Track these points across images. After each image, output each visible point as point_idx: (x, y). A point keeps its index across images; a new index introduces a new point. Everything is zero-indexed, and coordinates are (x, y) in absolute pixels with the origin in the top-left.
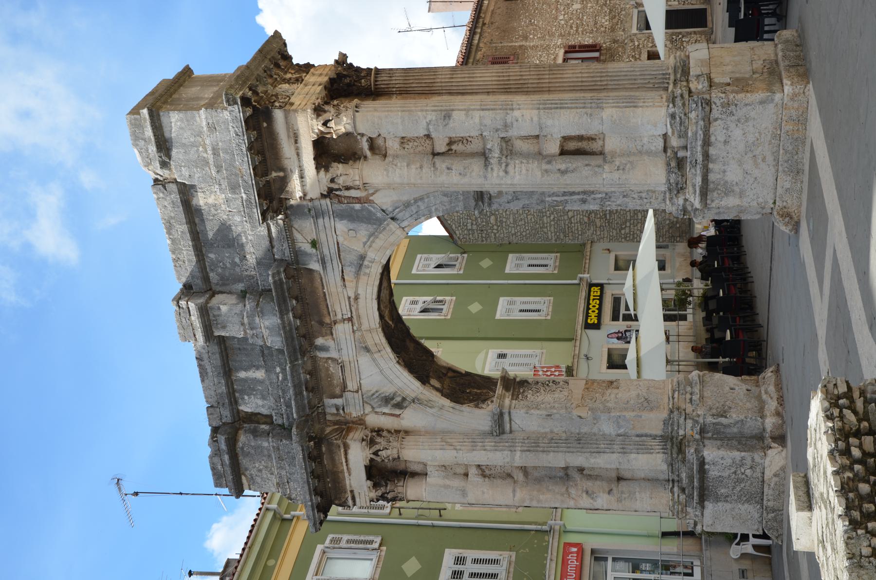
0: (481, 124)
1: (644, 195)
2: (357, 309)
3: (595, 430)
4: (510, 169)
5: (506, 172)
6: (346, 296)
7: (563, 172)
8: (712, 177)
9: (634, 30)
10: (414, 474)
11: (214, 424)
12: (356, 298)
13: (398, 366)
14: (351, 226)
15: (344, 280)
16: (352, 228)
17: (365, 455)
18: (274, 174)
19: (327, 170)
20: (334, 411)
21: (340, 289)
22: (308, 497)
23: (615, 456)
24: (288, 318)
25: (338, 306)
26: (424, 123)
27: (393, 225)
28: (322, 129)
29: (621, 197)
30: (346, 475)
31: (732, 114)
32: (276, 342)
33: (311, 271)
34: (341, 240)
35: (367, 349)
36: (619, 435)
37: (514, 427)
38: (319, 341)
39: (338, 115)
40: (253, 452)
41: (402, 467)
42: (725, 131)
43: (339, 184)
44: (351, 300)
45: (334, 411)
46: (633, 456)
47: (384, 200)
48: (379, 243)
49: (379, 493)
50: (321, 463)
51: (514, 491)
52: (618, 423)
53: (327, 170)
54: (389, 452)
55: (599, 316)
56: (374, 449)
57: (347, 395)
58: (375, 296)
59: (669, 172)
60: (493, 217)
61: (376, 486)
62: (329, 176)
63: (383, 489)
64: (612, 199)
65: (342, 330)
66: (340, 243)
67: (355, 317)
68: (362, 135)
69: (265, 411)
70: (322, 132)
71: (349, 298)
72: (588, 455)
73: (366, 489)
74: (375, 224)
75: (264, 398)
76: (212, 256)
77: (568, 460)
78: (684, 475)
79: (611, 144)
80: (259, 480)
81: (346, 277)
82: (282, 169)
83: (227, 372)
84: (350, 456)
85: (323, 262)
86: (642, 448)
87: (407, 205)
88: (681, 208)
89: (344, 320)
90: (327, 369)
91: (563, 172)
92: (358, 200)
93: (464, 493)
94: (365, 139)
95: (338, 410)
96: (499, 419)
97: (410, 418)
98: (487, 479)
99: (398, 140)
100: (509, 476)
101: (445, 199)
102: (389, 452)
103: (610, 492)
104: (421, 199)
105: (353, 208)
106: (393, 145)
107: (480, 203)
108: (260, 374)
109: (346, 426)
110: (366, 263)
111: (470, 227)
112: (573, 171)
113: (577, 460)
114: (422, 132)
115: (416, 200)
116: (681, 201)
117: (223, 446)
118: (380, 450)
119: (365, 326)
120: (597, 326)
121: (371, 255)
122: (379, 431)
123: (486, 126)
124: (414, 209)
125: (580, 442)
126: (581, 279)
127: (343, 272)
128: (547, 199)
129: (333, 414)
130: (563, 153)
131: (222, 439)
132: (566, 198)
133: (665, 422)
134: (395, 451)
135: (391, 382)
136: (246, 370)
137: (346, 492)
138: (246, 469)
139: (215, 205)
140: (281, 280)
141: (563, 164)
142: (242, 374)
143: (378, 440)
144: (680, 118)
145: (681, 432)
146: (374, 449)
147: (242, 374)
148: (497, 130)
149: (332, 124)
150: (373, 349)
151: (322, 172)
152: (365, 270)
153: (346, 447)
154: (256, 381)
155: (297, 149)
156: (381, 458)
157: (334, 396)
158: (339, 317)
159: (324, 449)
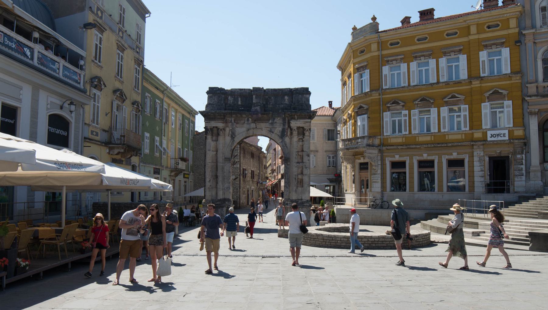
4: (296, 168)
5: (296, 167)
7: (295, 179)
9: (247, 187)
10: (212, 138)
14: (281, 131)
18: (296, 117)
19: (297, 129)
20: (230, 120)
23: (222, 187)
26: (307, 151)
27: (281, 141)
31: (308, 212)
33: (269, 120)
35: (248, 130)
38: (250, 119)
40: (220, 99)
41: (213, 135)
45: (230, 120)
46: (222, 191)
47: (287, 139)
49: (209, 129)
51: (210, 163)
53: (297, 129)
54: (221, 133)
55: (186, 178)
57: (235, 124)
59: (295, 200)
60: (203, 147)
61: (211, 129)
62: (295, 129)
63: (210, 130)
65: (253, 125)
68: (304, 137)
69: (229, 102)
70: (305, 129)
75: (233, 103)
76: (272, 98)
78: (218, 203)
80: (211, 99)
82: (297, 119)
84: (220, 123)
86: (224, 193)
87: (286, 144)
90: (242, 120)
91: (295, 179)
92: (287, 134)
93: (209, 150)
97: (228, 139)
101: (287, 152)
102: (221, 133)
103: (210, 186)
104: (287, 147)
108: (240, 103)
109: (226, 122)
110: (271, 133)
112: (296, 181)
113: (220, 179)
114: (304, 150)
115: (287, 147)
120: (184, 177)
121: (273, 135)
122: (225, 131)
126: (191, 172)
130: (298, 178)
136: (241, 100)
138: (214, 96)
139: (285, 101)
142: (240, 99)
145: (227, 202)
147: (240, 99)
150: (248, 132)
151: (296, 128)
153: (223, 123)
154: (238, 102)
157: (234, 121)
159: (222, 117)
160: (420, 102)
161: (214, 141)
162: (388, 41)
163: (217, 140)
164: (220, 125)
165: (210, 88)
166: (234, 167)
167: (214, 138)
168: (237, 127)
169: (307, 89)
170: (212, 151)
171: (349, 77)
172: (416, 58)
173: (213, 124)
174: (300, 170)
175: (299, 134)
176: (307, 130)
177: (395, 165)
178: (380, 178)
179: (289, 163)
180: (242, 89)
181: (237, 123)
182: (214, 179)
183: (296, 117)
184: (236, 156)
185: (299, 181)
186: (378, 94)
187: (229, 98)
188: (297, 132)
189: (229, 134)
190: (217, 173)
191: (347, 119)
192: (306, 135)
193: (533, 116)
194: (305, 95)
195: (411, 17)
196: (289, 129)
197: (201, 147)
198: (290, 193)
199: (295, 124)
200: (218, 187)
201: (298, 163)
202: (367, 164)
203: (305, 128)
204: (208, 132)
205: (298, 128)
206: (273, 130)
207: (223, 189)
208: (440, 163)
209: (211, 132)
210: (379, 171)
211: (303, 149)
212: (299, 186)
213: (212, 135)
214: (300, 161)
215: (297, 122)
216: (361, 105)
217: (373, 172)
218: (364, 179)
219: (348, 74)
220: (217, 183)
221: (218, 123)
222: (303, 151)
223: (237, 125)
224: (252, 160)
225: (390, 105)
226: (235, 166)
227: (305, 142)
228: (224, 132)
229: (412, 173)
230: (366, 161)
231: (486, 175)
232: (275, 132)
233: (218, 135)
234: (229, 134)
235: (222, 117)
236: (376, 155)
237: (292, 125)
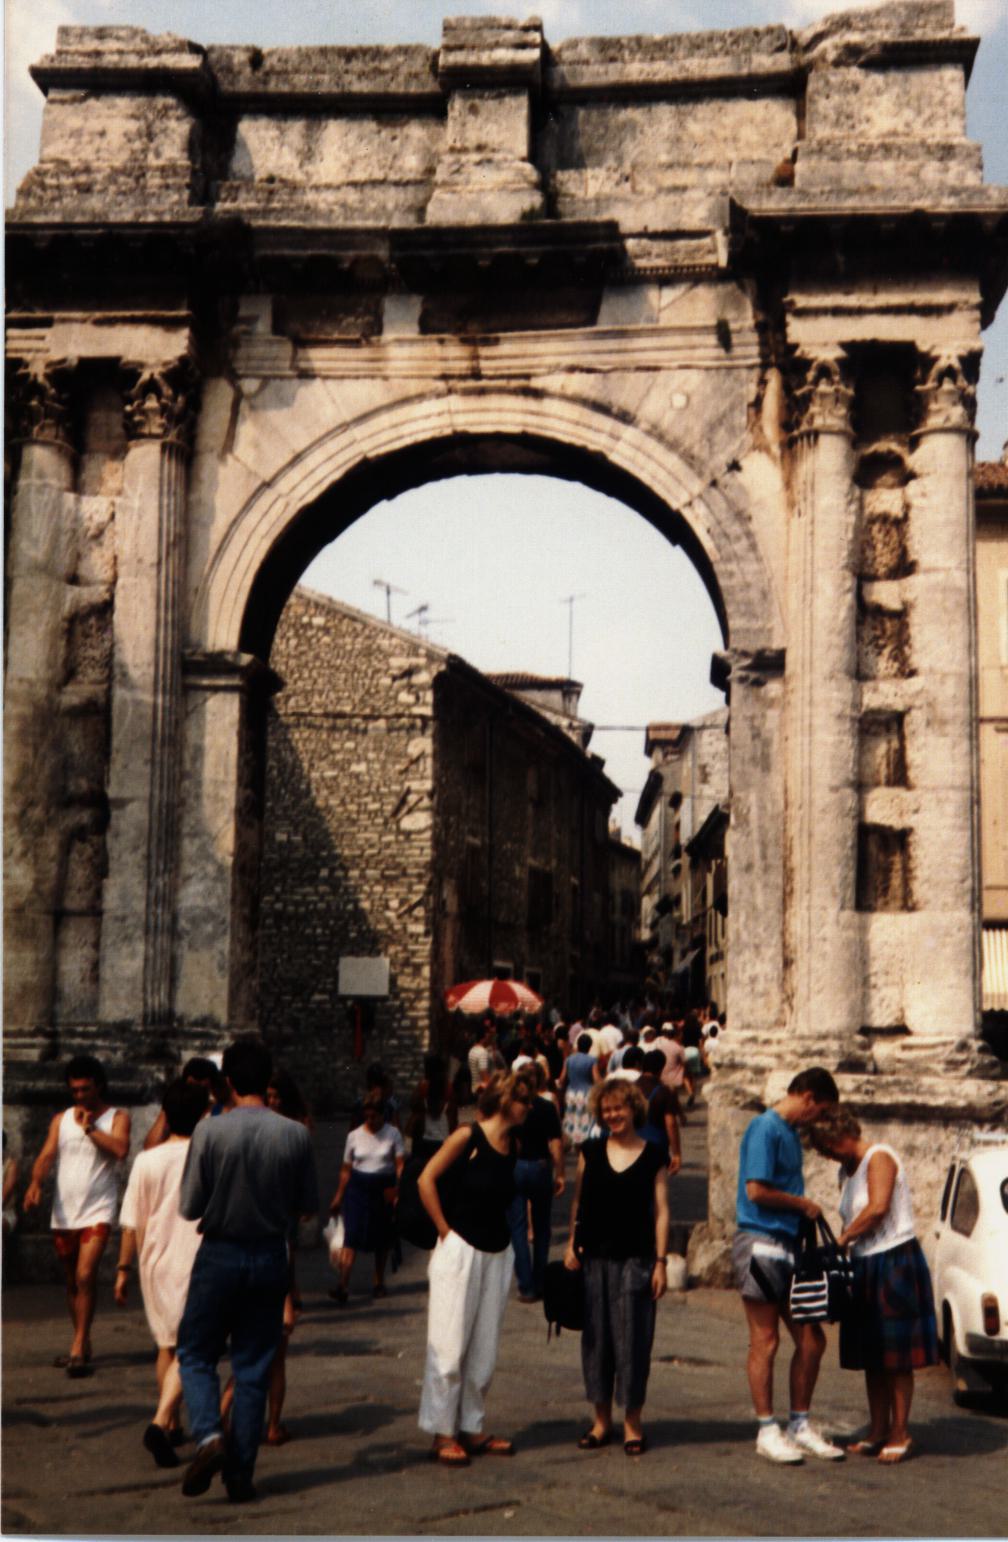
0: (945, 675)
1: (760, 987)
2: (501, 391)
3: (188, 869)
6: (532, 371)
11: (213, 56)
13: (358, 459)
15: (572, 369)
16: (695, 400)
17: (151, 360)
21: (550, 360)
24: (500, 243)
28: (942, 363)
29: (757, 941)
30: (98, 315)
32: (444, 210)
36: (175, 918)
37: (198, 697)
42: (935, 1146)
43: (816, 382)
44: (522, 383)
46: (140, 947)
52: (206, 920)
57: (286, 349)
63: (53, 391)
64: (751, 924)
66: (661, 376)
67: (483, 383)
71: (527, 377)
72: (143, 850)
73: (56, 355)
74: (702, 447)
77: (131, 807)
79: (886, 926)
81: (577, 377)
87: (742, 517)
88: (738, 1059)
90: (349, 311)
94: (894, 447)
96: (217, 663)
98: (65, 625)
99: (896, 510)
101: (754, 594)
104: (753, 547)
106: (885, 499)
107: (747, 662)
115: (749, 535)
116: (751, 1061)
117: (170, 61)
118: (159, 396)
119: (455, 402)
121: (628, 433)
123: (942, 682)
124: (735, 529)
127: (590, 371)
128: (753, 798)
131: (190, 61)
132: (755, 835)
133: (207, 1021)
134: (156, 430)
135: (318, 442)
137: (46, 308)
140: (596, 239)
143: (180, 399)
144: (963, 1062)
148: (930, 705)
149: (947, 386)
151: (839, 353)
153: (171, 325)
156: (136, 398)
158: (484, 351)
166: (399, 832)
179: (773, 688)
181: (301, 343)
183: (841, 258)
184: (415, 761)
190: (101, 779)
192: (934, 421)
196: (774, 379)
198: (787, 963)
200: (111, 900)
205: (862, 359)
206: (625, 391)
207: (150, 930)
211: (904, 551)
222: (904, 568)
224: (530, 810)
226: (407, 823)
237: (798, 330)
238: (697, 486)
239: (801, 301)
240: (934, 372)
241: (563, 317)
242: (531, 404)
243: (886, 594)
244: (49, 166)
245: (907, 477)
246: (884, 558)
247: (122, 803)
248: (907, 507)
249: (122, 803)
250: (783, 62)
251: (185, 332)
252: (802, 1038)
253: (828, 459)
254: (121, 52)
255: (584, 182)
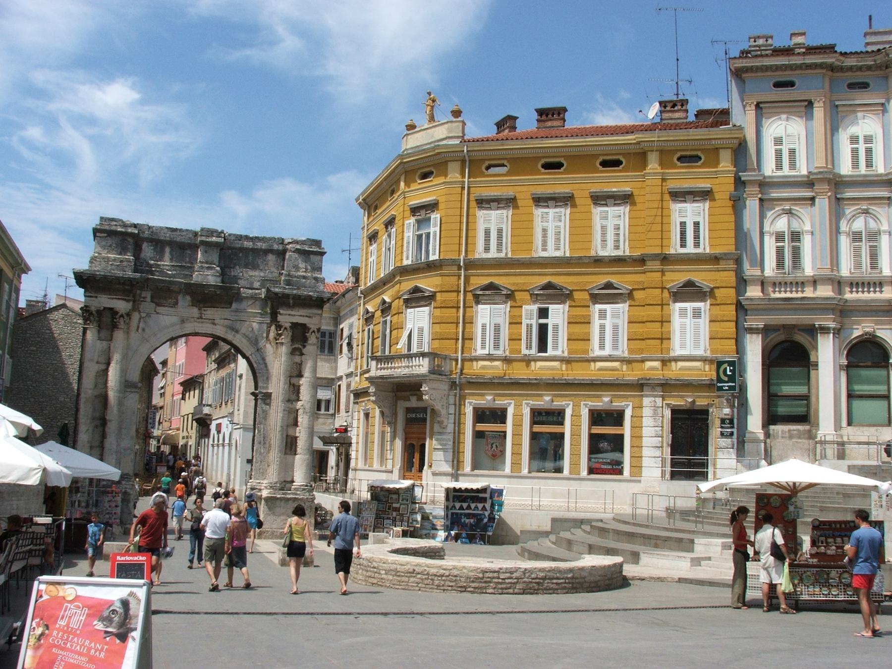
1: (261, 471)
2: (207, 323)
8: (279, 501)
10: (99, 332)
12: (214, 324)
19: (290, 327)
22: (103, 273)
23: (115, 447)
25: (210, 313)
33: (231, 304)
34: (248, 323)
35: (183, 321)
37: (127, 394)
38: (188, 298)
39: (317, 338)
46: (114, 456)
48: (245, 341)
49: (94, 313)
50: (119, 284)
51: (90, 389)
54: (122, 323)
56: (125, 317)
57: (153, 305)
58: (214, 333)
60: (35, 349)
65: (195, 311)
68: (304, 347)
76: (241, 255)
83: (172, 243)
85: (237, 311)
87: (264, 359)
89: (201, 314)
90: (171, 298)
92: (267, 337)
93: (92, 360)
95: (144, 298)
99: (299, 361)
100: (96, 386)
102: (122, 323)
104: (266, 366)
105: (263, 332)
106: (297, 359)
111: (28, 332)
113: (112, 427)
115: (266, 364)
117: (130, 230)
121: (238, 336)
124: (261, 362)
125: (120, 429)
129: (140, 294)
130: (287, 436)
136: (171, 253)
141: (285, 436)
142: (168, 250)
146: (125, 317)
147: (168, 250)
152: (229, 331)
153: (128, 301)
155: (303, 316)
157: (152, 298)
159: (127, 287)
160: (541, 292)
161: (103, 340)
162: (484, 160)
163: (111, 340)
164: (121, 306)
165: (102, 218)
167: (104, 333)
168: (158, 313)
169: (318, 243)
170: (97, 363)
171: (390, 223)
172: (539, 202)
173: (104, 301)
174: (292, 416)
175: (293, 340)
176: (314, 331)
177: (481, 415)
178: (451, 443)
179: (268, 401)
180: (175, 230)
181: (158, 305)
182: (96, 427)
185: (289, 440)
186: (456, 268)
187: (145, 246)
188: (291, 334)
189: (138, 327)
191: (374, 313)
192: (309, 342)
193: (754, 336)
194: (312, 256)
195: (518, 118)
196: (273, 328)
197: (32, 348)
199: (287, 317)
201: (289, 401)
202: (424, 410)
203: (311, 326)
204: (92, 318)
205: (295, 326)
207: (117, 452)
208: (576, 415)
209: (97, 319)
210: (450, 428)
211: (300, 372)
212: (288, 451)
213: (99, 326)
214: (293, 397)
215: (293, 313)
216: (416, 286)
217: (436, 428)
218: (414, 443)
219: (386, 217)
220: (103, 436)
221: (115, 301)
223: (159, 309)
225: (481, 293)
227: (308, 357)
228: (127, 321)
229: (517, 435)
230: (420, 404)
231: (665, 445)
232: (243, 330)
233: (114, 326)
234: (138, 327)
235: (127, 287)
236: (446, 393)
237: (280, 318)
238: (253, 350)
239: (282, 311)
240: (311, 331)
241: (223, 306)
242: (214, 326)
243: (294, 381)
244: (96, 255)
245: (302, 354)
246: (295, 373)
247: (110, 421)
248: (302, 361)
249: (110, 421)
250: (281, 247)
251: (131, 303)
252: (271, 483)
253: (284, 350)
254: (116, 225)
255: (231, 272)
